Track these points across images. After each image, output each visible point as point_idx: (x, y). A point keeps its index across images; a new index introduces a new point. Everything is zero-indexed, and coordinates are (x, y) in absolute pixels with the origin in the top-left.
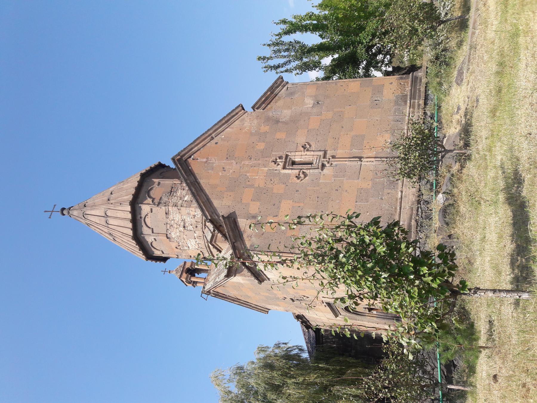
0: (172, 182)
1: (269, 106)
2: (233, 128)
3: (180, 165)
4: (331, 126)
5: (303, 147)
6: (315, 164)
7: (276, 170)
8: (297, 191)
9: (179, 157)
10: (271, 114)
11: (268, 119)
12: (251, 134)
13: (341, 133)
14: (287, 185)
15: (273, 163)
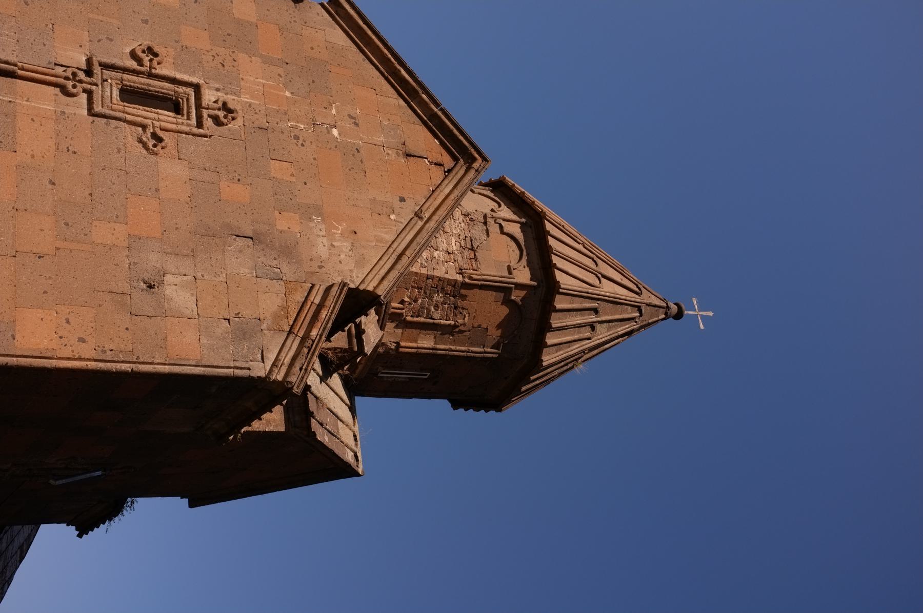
0: (484, 272)
1: (300, 297)
2: (380, 240)
3: (461, 142)
4: (90, 195)
5: (160, 140)
6: (114, 84)
7: (218, 90)
8: (146, 22)
9: (476, 165)
10: (285, 268)
11: (288, 251)
12: (318, 210)
13: (53, 164)
14: (177, 42)
15: (231, 106)
